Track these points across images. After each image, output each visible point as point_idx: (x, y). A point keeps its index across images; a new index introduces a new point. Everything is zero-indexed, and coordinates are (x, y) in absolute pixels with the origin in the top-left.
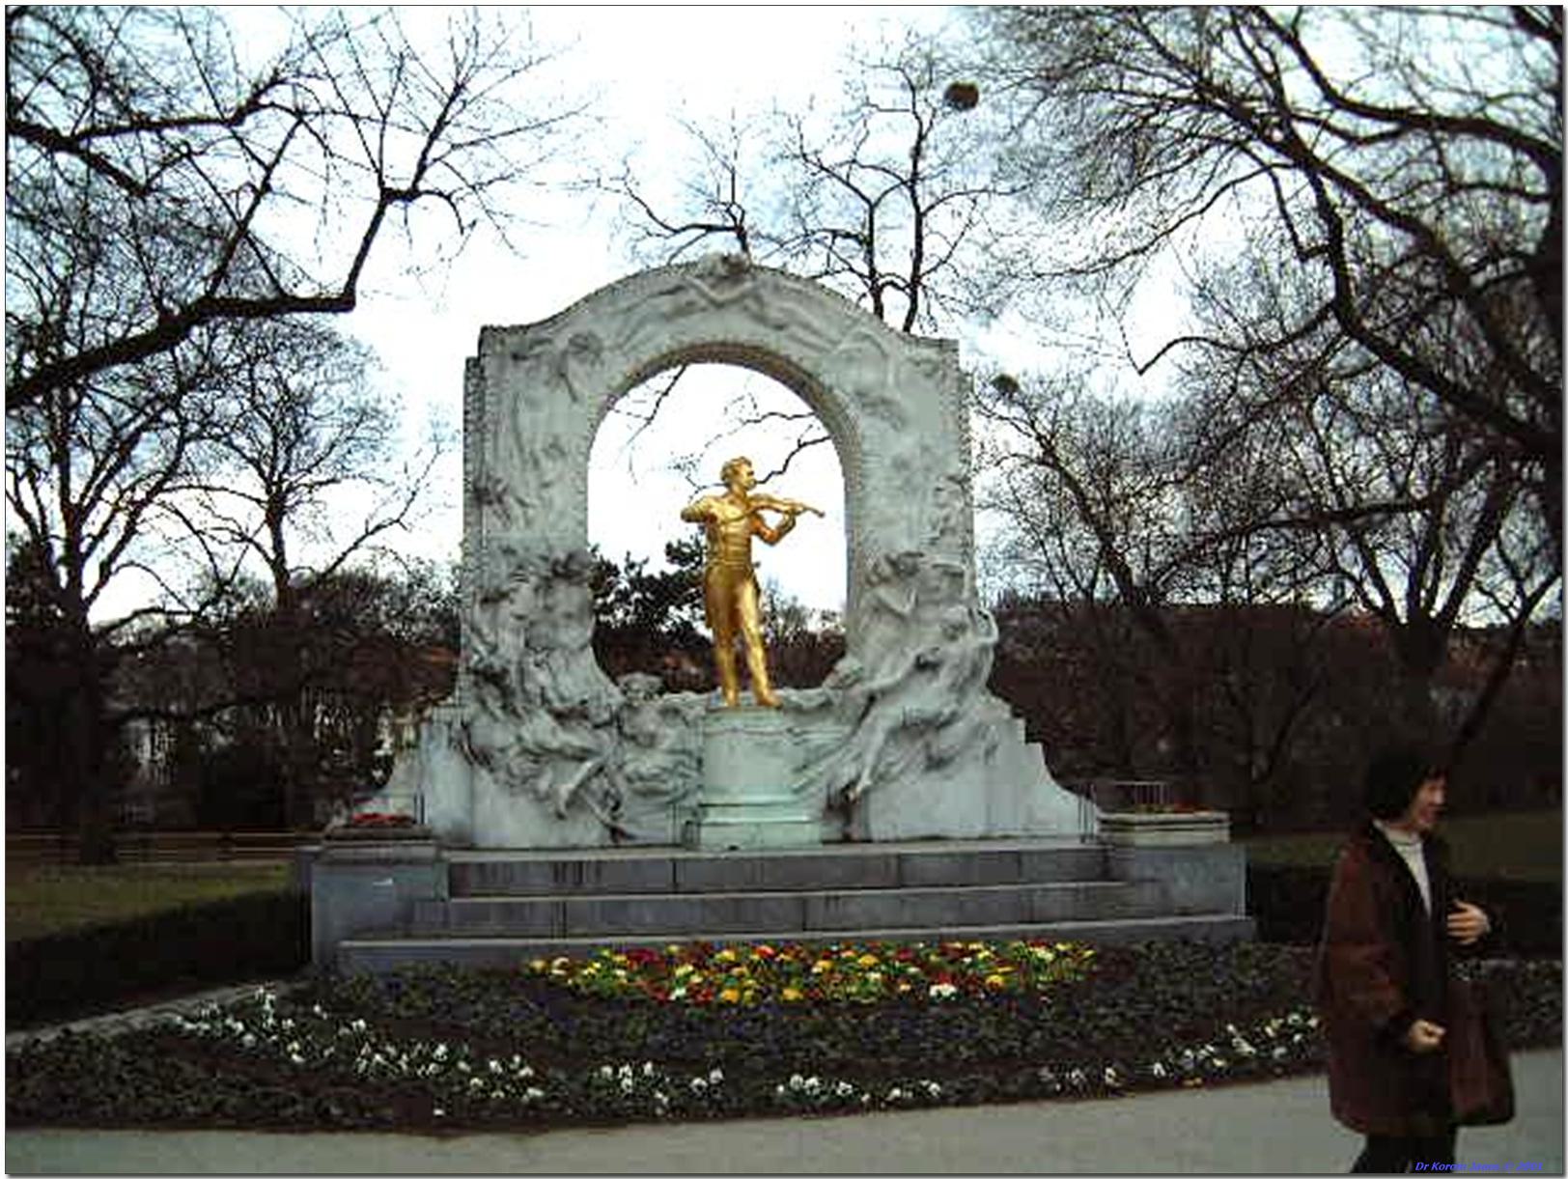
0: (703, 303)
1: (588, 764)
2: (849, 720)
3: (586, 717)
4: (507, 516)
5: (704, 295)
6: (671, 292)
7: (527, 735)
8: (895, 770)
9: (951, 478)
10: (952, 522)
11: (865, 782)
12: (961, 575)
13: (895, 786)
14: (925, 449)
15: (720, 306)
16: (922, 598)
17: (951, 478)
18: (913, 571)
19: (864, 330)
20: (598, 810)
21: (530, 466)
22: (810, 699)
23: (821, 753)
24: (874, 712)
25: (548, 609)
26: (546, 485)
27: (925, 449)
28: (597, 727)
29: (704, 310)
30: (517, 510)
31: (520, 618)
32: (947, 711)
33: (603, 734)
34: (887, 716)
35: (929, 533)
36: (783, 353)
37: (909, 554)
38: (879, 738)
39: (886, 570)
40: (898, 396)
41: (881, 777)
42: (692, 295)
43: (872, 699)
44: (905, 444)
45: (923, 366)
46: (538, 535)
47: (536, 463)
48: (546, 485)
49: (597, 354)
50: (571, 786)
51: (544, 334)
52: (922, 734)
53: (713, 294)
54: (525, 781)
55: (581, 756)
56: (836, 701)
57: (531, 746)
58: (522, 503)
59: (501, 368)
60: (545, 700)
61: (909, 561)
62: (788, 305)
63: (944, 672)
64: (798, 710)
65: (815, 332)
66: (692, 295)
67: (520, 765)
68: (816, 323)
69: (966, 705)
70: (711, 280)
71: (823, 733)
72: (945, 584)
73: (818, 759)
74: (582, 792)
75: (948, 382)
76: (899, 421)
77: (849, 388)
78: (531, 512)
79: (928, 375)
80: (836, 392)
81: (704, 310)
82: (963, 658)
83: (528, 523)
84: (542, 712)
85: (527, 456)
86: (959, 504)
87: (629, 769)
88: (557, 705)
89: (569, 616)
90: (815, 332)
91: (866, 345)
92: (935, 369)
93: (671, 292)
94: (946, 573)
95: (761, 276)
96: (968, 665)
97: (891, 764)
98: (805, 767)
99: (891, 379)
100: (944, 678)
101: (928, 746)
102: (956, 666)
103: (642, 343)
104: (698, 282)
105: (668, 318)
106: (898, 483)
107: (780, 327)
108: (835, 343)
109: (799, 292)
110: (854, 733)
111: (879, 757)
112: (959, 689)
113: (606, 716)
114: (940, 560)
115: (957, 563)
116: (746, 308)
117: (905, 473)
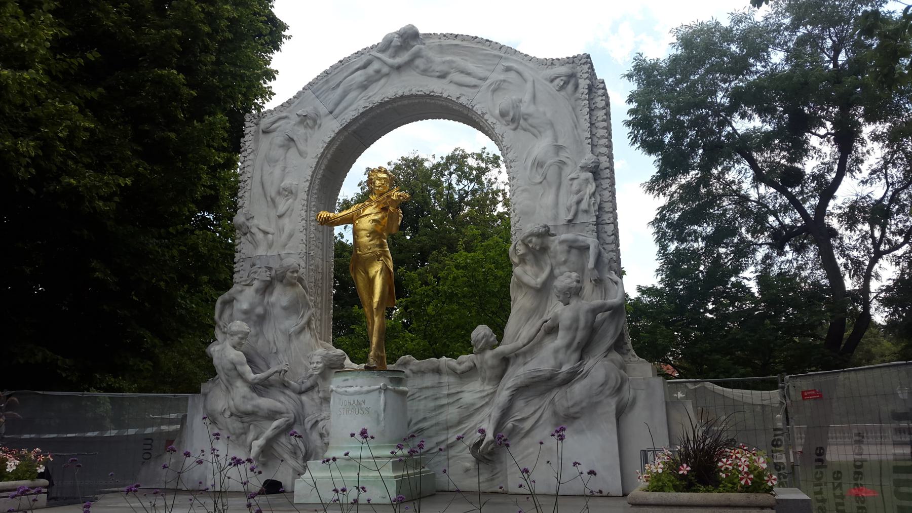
0: (385, 70)
1: (275, 424)
2: (490, 380)
3: (285, 385)
4: (255, 244)
5: (385, 63)
6: (365, 66)
7: (232, 403)
8: (527, 425)
9: (583, 168)
10: (584, 205)
11: (490, 436)
12: (588, 248)
13: (525, 441)
14: (558, 148)
15: (399, 68)
16: (557, 271)
17: (583, 168)
18: (544, 249)
19: (506, 64)
20: (292, 462)
21: (270, 203)
22: (460, 364)
23: (470, 412)
24: (510, 370)
25: (273, 305)
26: (280, 217)
27: (558, 148)
28: (301, 393)
29: (387, 75)
30: (260, 236)
31: (246, 312)
32: (565, 368)
33: (304, 398)
34: (517, 374)
35: (564, 217)
36: (445, 95)
37: (532, 235)
38: (503, 396)
39: (521, 250)
40: (531, 109)
41: (514, 431)
42: (376, 66)
43: (505, 361)
44: (541, 146)
45: (558, 80)
46: (275, 253)
47: (273, 201)
48: (280, 217)
49: (315, 121)
50: (261, 441)
51: (284, 114)
52: (550, 390)
53: (390, 61)
54: (238, 436)
55: (272, 415)
56: (478, 365)
57: (234, 410)
58: (266, 233)
59: (257, 141)
60: (241, 376)
61: (534, 239)
62: (448, 58)
63: (561, 333)
64: (453, 372)
65: (469, 74)
66: (376, 66)
67: (236, 425)
68: (471, 66)
69: (589, 363)
70: (391, 50)
71: (473, 391)
72: (574, 256)
73: (470, 416)
74: (275, 446)
75: (581, 90)
76: (535, 131)
77: (497, 112)
78: (270, 236)
79: (562, 88)
80: (486, 117)
81: (387, 75)
82: (576, 320)
83: (270, 246)
84: (239, 383)
85: (269, 199)
86: (591, 188)
87: (320, 424)
88: (251, 376)
89: (285, 308)
90: (469, 74)
91: (512, 76)
92: (566, 83)
93: (365, 66)
94: (571, 247)
95: (427, 42)
96: (582, 323)
97: (523, 420)
98: (460, 423)
99: (527, 97)
100: (560, 340)
101: (552, 402)
102: (573, 326)
103: (346, 108)
104: (379, 55)
105: (364, 87)
106: (538, 179)
107: (443, 76)
108: (484, 79)
109: (456, 45)
110: (495, 392)
111: (506, 413)
112: (584, 349)
113: (308, 383)
114: (564, 236)
115: (581, 238)
116: (417, 67)
117: (541, 171)
